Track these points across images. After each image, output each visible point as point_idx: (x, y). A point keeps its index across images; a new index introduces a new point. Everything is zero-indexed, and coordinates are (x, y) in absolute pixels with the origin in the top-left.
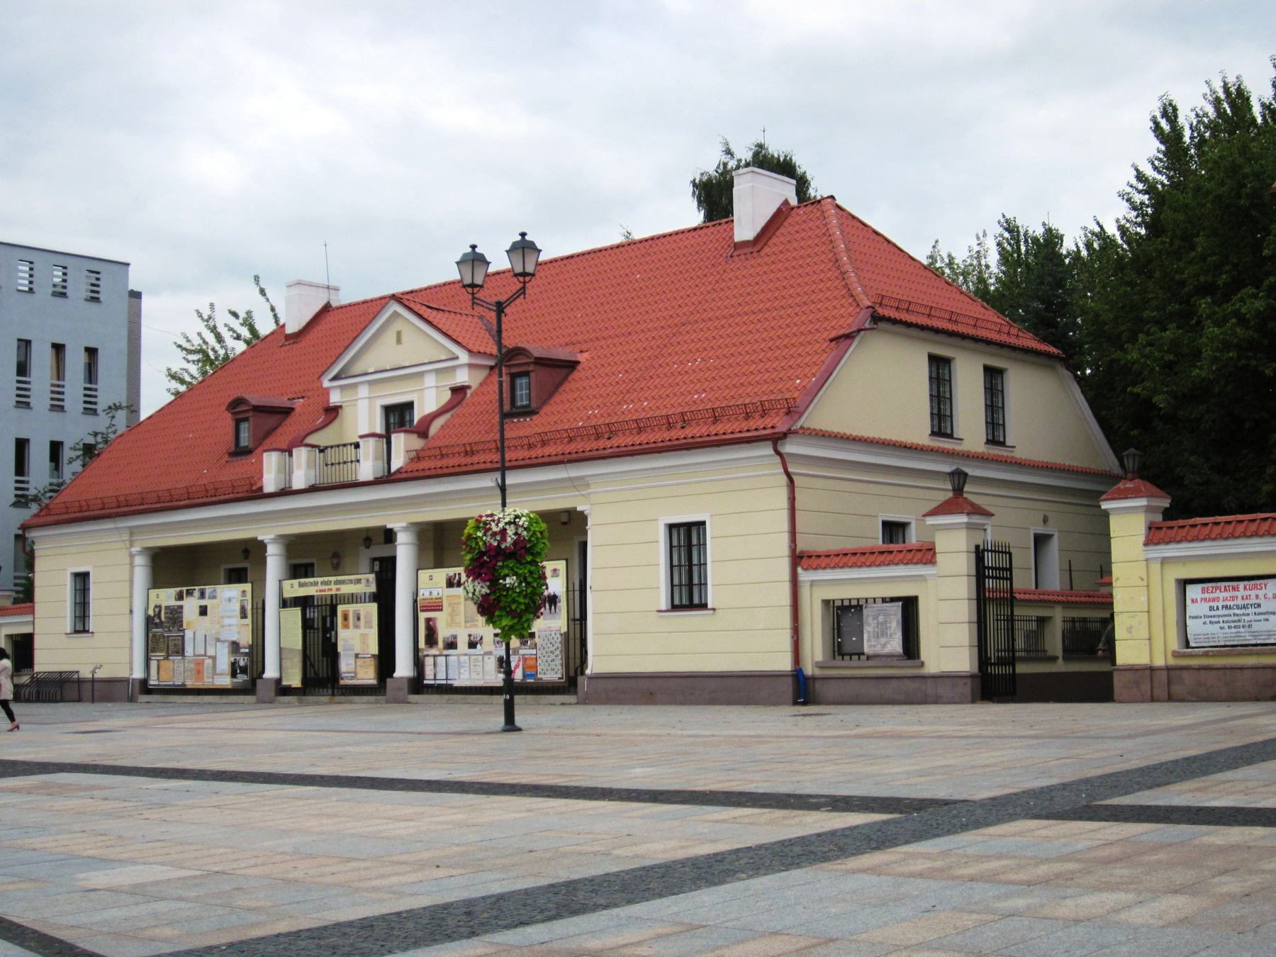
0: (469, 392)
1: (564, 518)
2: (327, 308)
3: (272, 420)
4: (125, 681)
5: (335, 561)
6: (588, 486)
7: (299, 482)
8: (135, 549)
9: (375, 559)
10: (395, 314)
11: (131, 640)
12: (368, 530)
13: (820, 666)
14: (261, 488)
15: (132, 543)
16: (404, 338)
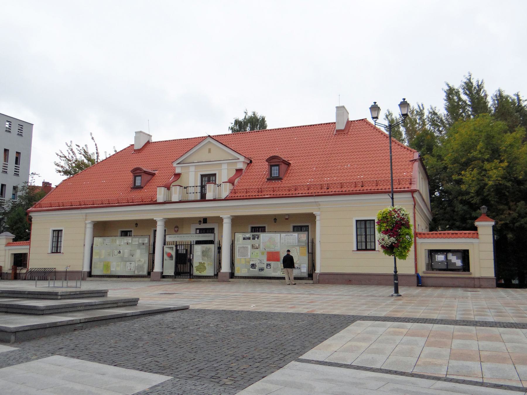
0: (243, 171)
1: (287, 217)
2: (148, 142)
3: (149, 177)
4: (81, 272)
5: (176, 229)
6: (320, 205)
7: (175, 198)
8: (87, 222)
9: (197, 229)
10: (209, 141)
11: (84, 256)
12: (200, 218)
13: (424, 273)
14: (156, 200)
15: (86, 219)
16: (212, 151)
